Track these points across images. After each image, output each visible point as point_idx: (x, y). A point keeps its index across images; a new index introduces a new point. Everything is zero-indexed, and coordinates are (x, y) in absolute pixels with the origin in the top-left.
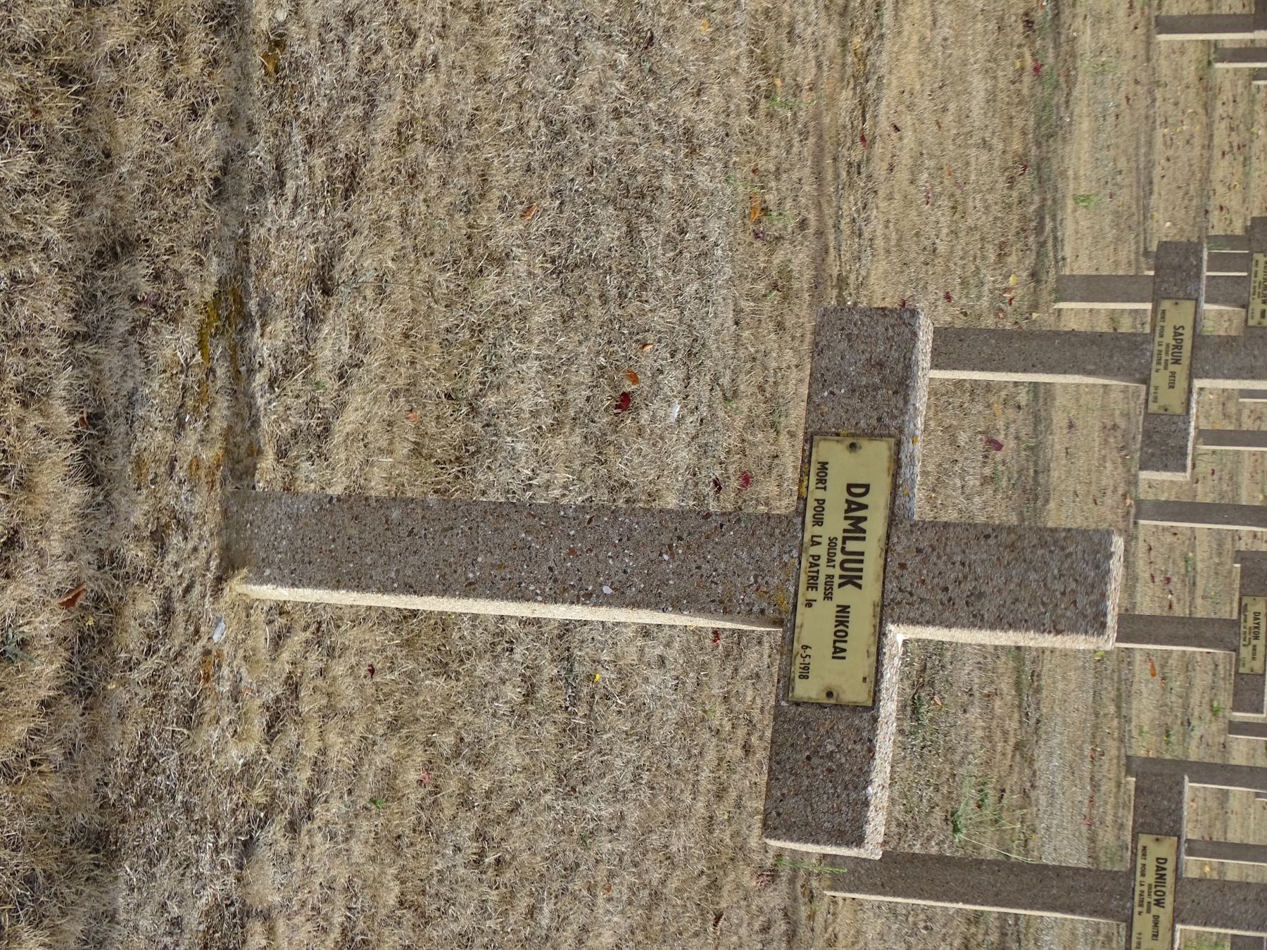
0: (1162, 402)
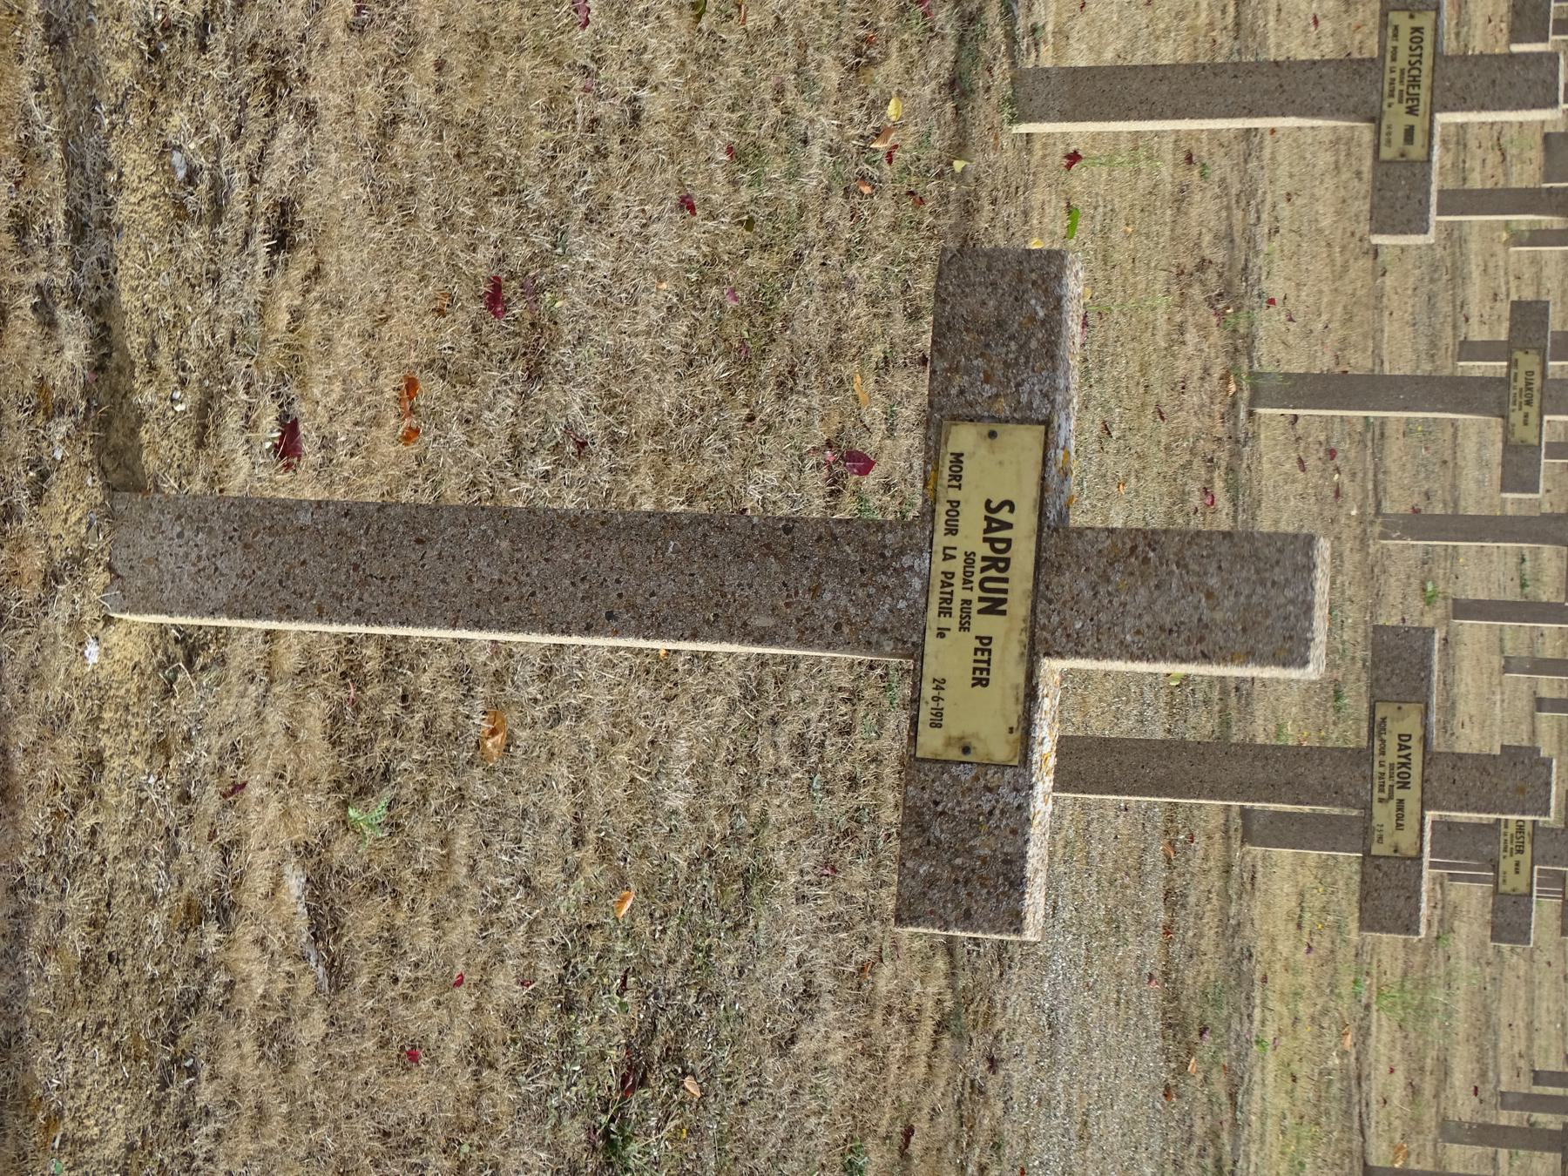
0: (954, 724)
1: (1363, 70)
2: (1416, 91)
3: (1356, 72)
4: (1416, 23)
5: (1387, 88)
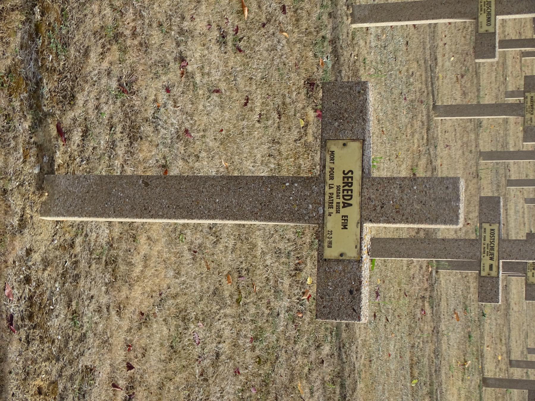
1: (474, 244)
2: (493, 252)
3: (471, 244)
4: (492, 228)
5: (482, 250)
